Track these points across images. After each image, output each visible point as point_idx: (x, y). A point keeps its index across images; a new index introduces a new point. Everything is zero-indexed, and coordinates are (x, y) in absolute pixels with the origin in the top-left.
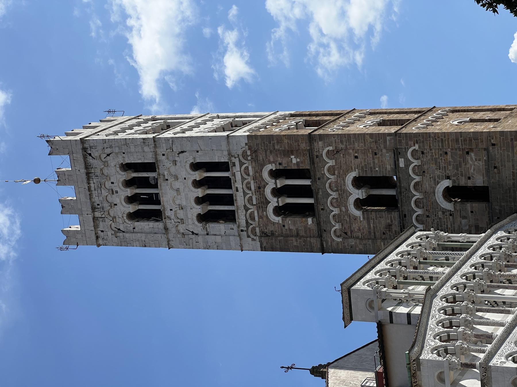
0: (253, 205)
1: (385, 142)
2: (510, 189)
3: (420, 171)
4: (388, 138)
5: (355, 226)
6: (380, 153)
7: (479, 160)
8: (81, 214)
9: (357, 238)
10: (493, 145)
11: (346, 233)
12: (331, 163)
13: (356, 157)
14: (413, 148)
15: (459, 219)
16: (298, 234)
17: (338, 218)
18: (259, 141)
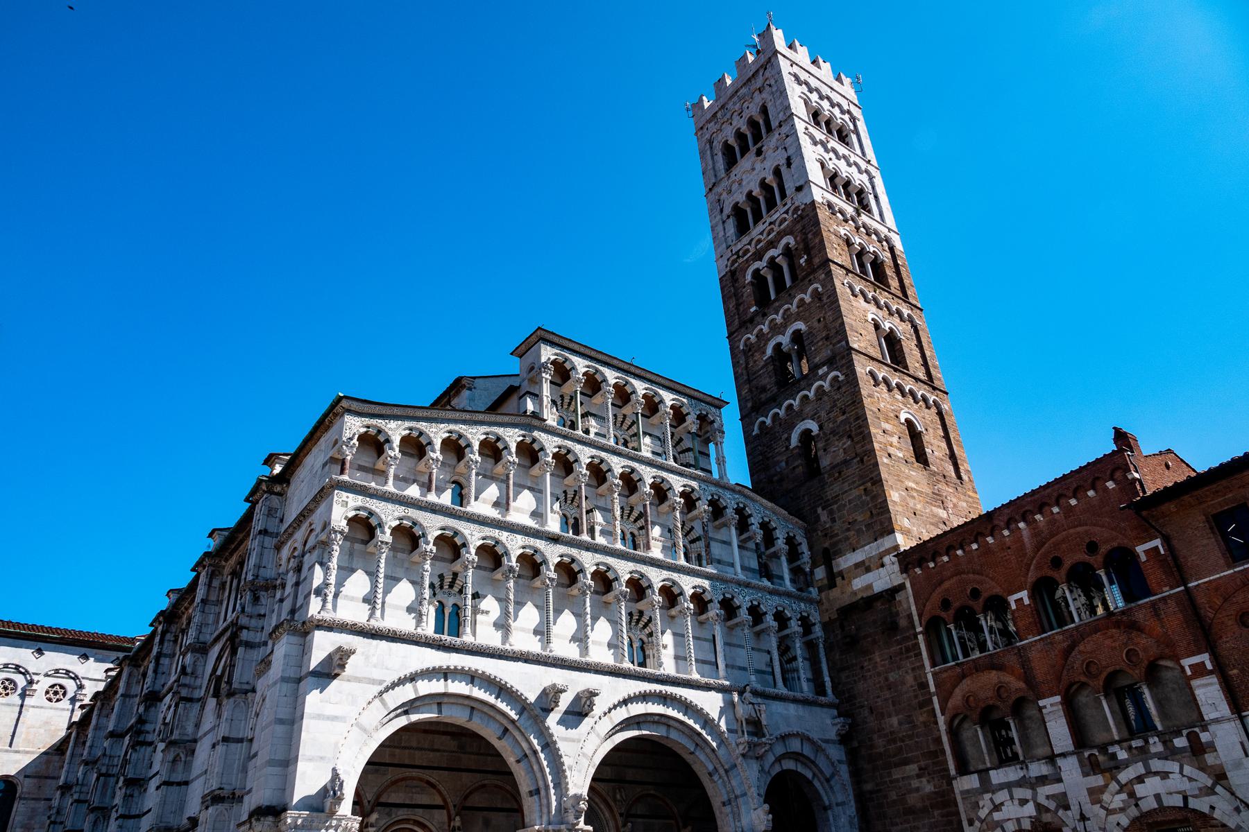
0: (756, 245)
1: (840, 341)
2: (822, 498)
3: (820, 391)
4: (844, 343)
5: (757, 356)
6: (828, 343)
7: (845, 453)
8: (716, 101)
9: (747, 363)
10: (862, 460)
11: (750, 350)
12: (808, 299)
13: (819, 321)
14: (839, 374)
15: (784, 458)
16: (740, 305)
17: (760, 335)
18: (811, 214)
